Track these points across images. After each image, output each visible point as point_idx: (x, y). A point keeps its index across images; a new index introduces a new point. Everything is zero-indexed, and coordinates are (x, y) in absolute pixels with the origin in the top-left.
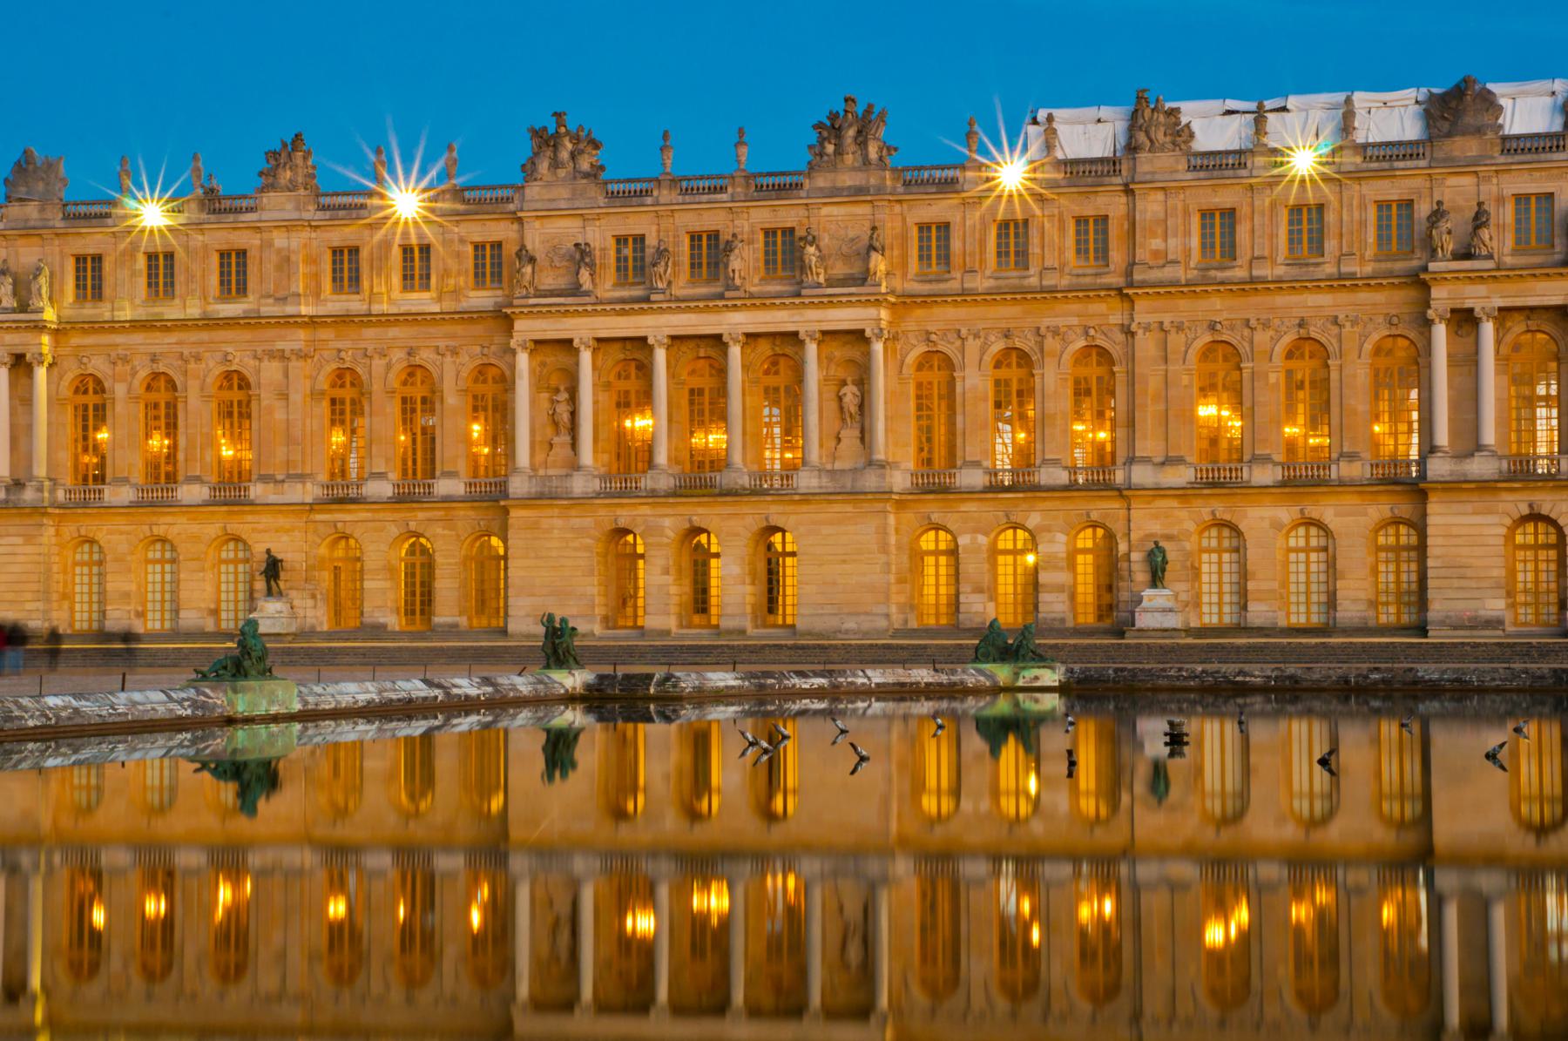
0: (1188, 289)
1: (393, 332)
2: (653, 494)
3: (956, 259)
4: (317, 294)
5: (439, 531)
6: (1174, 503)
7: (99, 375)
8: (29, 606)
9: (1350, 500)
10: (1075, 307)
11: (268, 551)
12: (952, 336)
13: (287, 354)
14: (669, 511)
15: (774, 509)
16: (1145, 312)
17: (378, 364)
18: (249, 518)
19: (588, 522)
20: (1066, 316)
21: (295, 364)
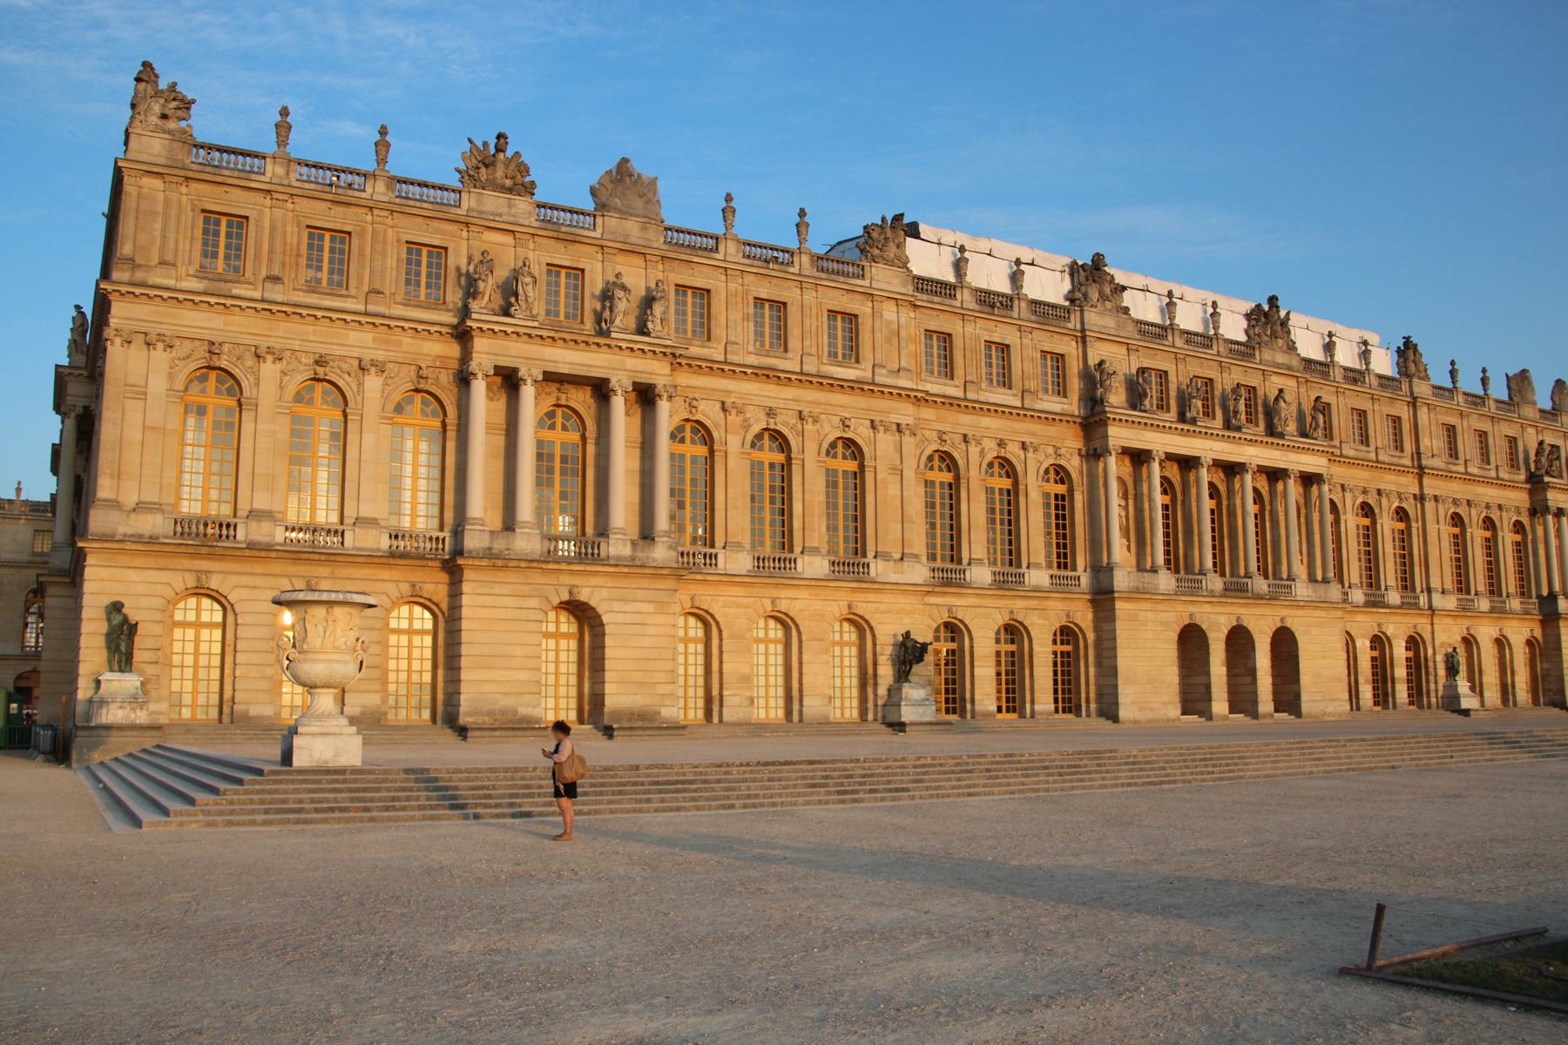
0: (1449, 476)
1: (986, 421)
2: (1212, 594)
3: (1336, 432)
4: (919, 374)
5: (1036, 620)
6: (1449, 621)
7: (707, 423)
8: (661, 689)
9: (1515, 623)
10: (1392, 477)
11: (908, 633)
12: (1339, 488)
13: (903, 427)
14: (1222, 610)
15: (1284, 612)
16: (1431, 486)
17: (974, 450)
18: (871, 597)
19: (1171, 616)
20: (1390, 482)
21: (907, 439)
